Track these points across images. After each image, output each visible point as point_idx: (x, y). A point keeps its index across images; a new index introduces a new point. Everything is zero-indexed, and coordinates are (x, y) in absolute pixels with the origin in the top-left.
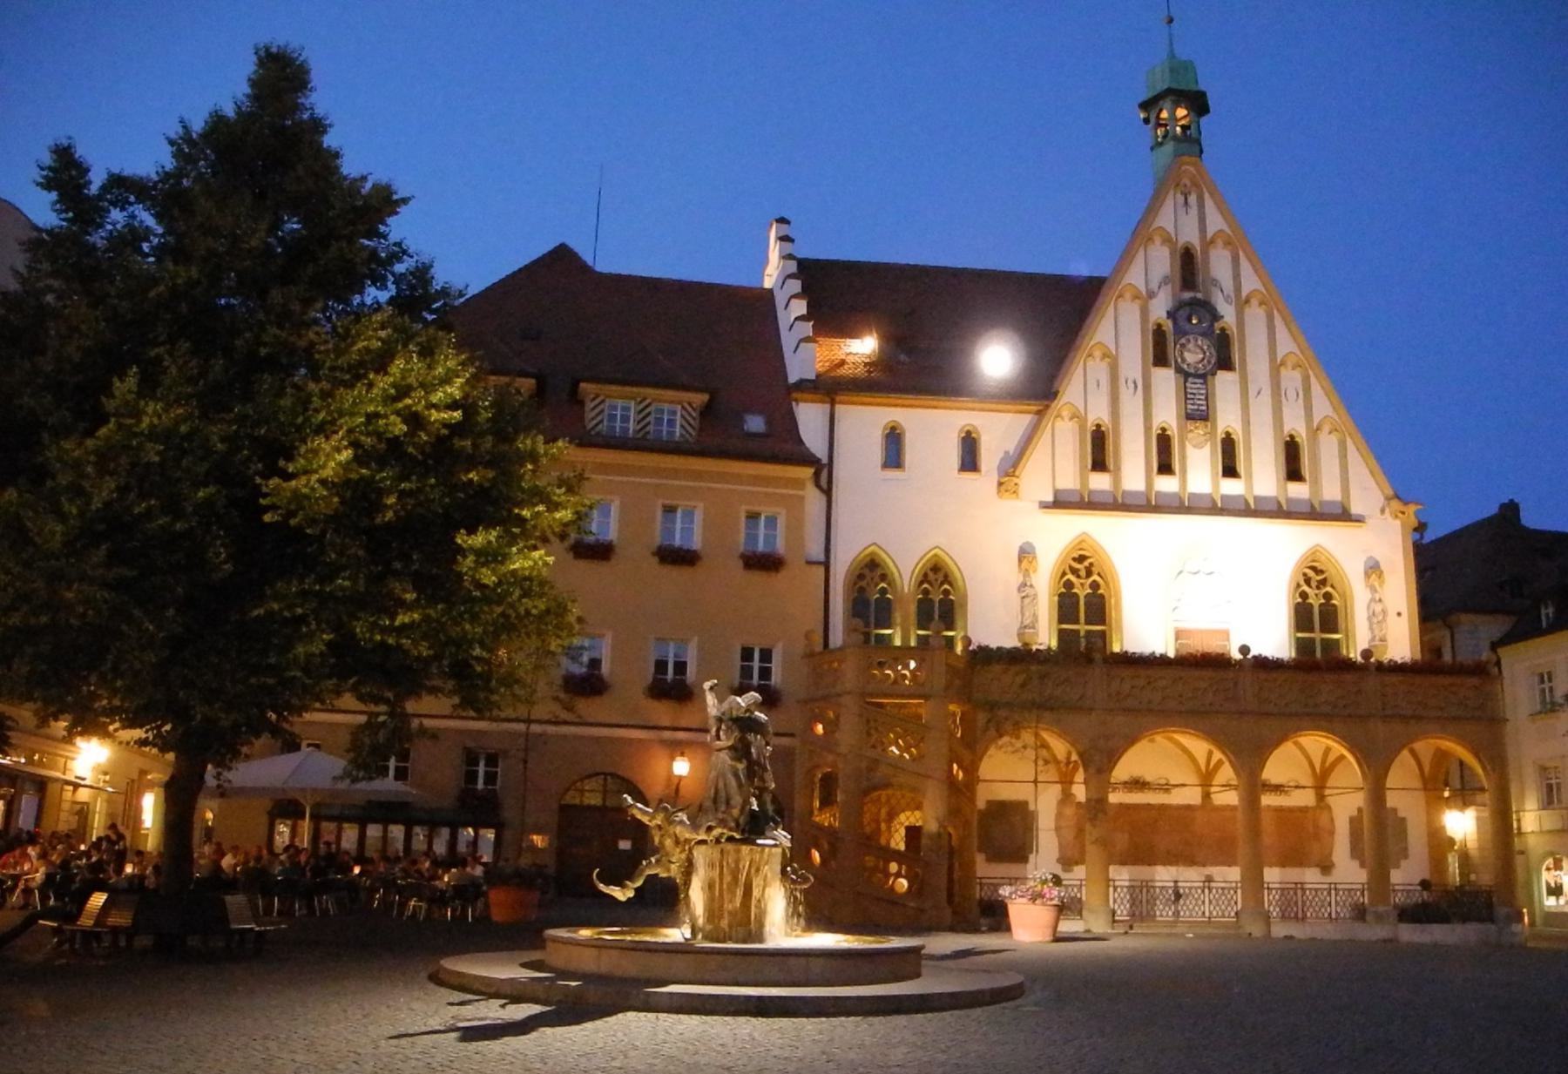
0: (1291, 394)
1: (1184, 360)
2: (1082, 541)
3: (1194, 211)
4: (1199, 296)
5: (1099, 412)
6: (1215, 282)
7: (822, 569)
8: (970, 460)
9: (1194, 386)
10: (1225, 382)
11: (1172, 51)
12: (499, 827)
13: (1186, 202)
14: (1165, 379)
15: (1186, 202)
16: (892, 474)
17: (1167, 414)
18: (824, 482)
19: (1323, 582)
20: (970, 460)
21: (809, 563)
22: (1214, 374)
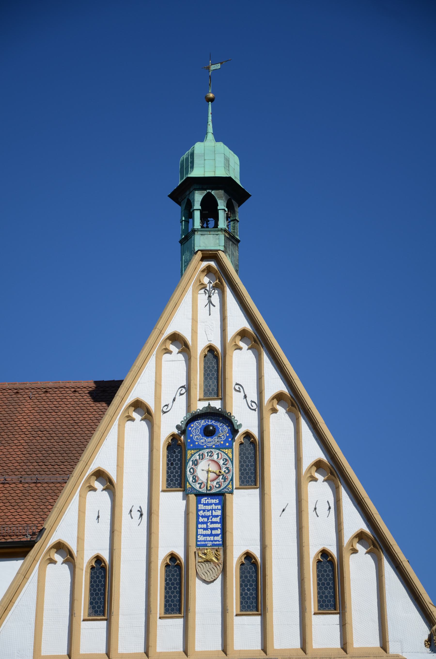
0: (323, 509)
1: (195, 479)
3: (216, 311)
4: (217, 404)
5: (97, 544)
6: (239, 388)
13: (210, 302)
14: (172, 505)
15: (210, 302)
22: (231, 493)
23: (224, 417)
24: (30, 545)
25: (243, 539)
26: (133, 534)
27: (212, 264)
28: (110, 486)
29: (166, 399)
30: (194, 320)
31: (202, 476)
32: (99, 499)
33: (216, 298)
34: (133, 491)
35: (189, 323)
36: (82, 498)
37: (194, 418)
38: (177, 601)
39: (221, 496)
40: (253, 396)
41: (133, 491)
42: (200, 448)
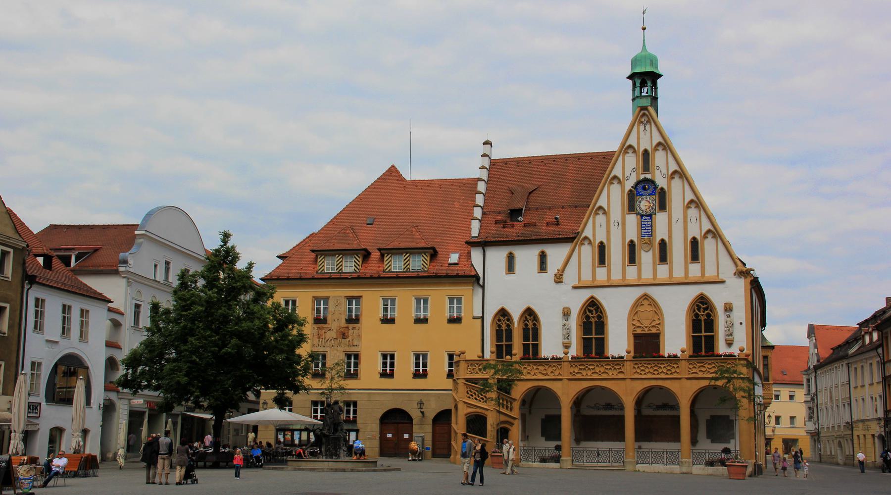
0: (694, 220)
2: (592, 297)
3: (648, 133)
4: (649, 176)
5: (601, 237)
7: (480, 320)
8: (543, 265)
11: (644, 46)
12: (357, 431)
17: (632, 233)
18: (481, 283)
19: (706, 309)
20: (543, 265)
21: (474, 318)
23: (652, 182)
24: (575, 238)
25: (661, 232)
26: (616, 232)
27: (646, 112)
29: (627, 174)
30: (638, 138)
31: (643, 208)
32: (601, 219)
35: (636, 140)
36: (594, 218)
38: (632, 260)
39: (650, 216)
40: (664, 171)
42: (642, 195)
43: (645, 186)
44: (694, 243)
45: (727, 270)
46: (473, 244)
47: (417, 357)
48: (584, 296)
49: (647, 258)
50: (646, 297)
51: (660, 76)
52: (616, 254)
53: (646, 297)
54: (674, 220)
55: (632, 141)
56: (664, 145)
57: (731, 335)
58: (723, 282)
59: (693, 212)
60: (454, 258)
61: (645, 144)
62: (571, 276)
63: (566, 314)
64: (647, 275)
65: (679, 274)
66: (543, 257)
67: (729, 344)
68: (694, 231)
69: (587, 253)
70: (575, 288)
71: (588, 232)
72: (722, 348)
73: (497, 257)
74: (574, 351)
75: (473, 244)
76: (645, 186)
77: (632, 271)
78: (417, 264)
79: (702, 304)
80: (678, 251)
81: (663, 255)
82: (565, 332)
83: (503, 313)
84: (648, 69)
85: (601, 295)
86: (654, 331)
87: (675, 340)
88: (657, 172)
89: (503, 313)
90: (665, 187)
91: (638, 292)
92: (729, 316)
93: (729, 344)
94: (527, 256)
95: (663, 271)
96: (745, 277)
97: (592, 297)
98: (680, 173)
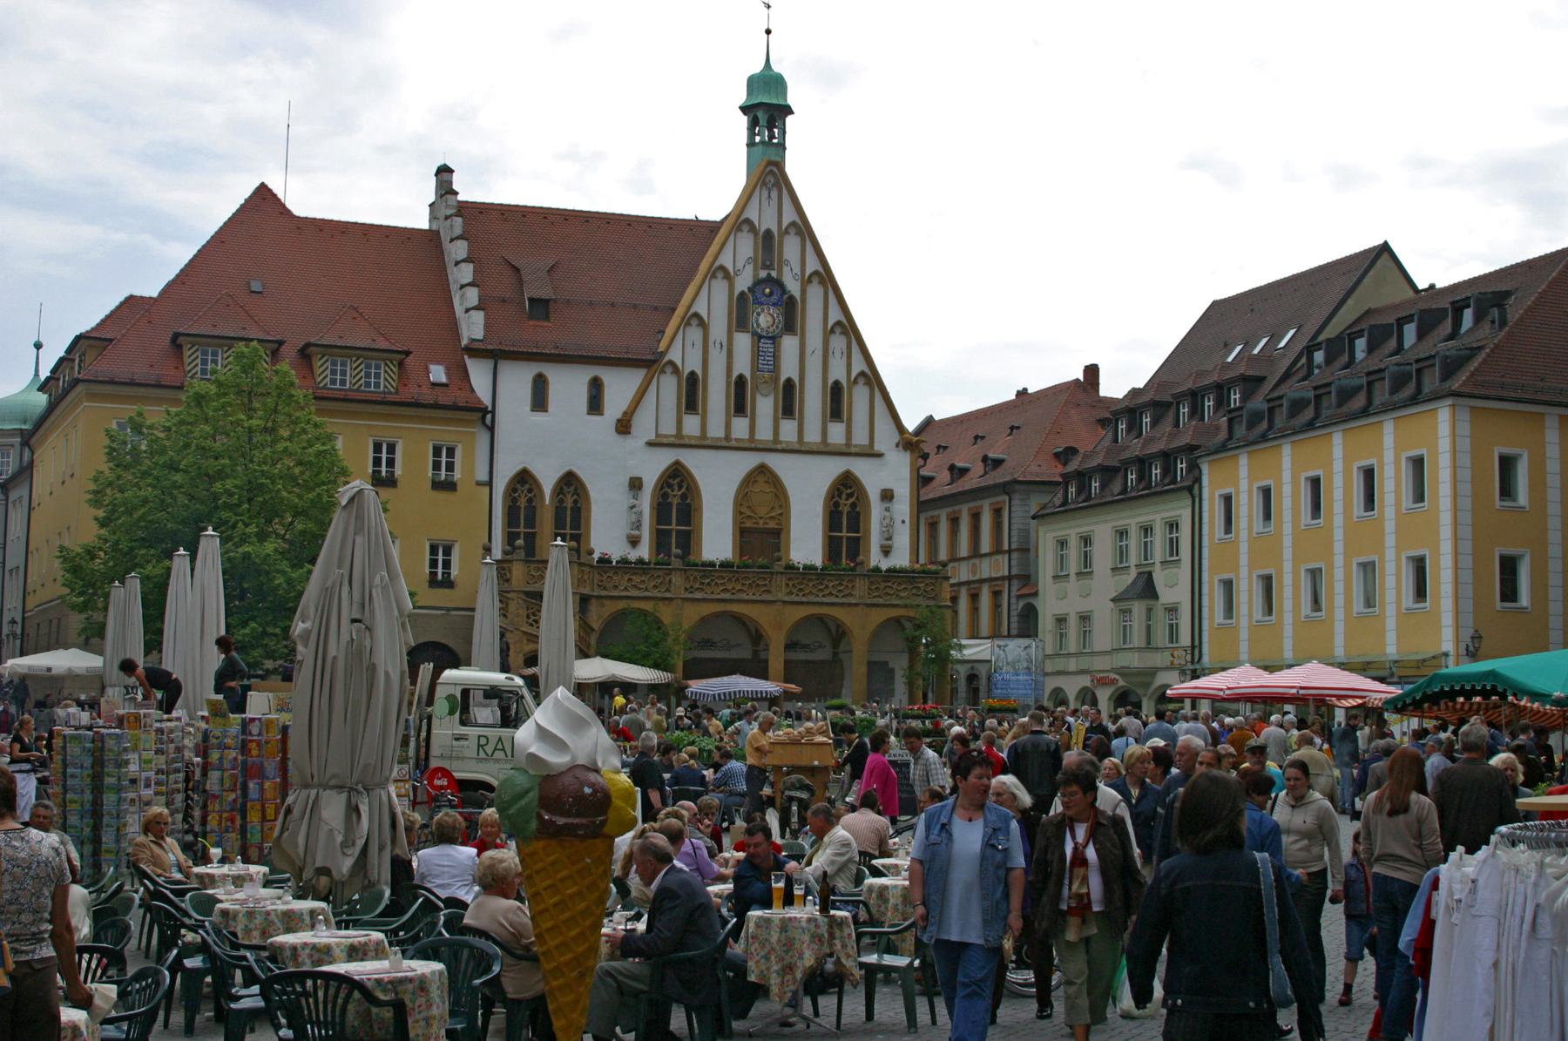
0: (838, 354)
2: (677, 463)
4: (774, 274)
5: (693, 364)
8: (595, 404)
9: (766, 346)
10: (789, 344)
16: (539, 417)
17: (743, 366)
19: (850, 496)
20: (595, 404)
21: (478, 484)
23: (779, 284)
25: (789, 369)
28: (703, 324)
29: (739, 265)
32: (695, 334)
33: (774, 194)
34: (719, 329)
37: (758, 283)
39: (774, 339)
40: (797, 270)
41: (719, 329)
43: (769, 288)
44: (836, 389)
45: (885, 439)
46: (474, 351)
47: (434, 550)
48: (662, 460)
49: (765, 406)
50: (762, 469)
51: (788, 110)
52: (717, 395)
53: (762, 469)
54: (808, 350)
55: (752, 213)
56: (803, 230)
57: (890, 538)
58: (880, 455)
59: (838, 342)
60: (438, 373)
61: (768, 222)
62: (644, 425)
63: (636, 485)
64: (764, 433)
65: (812, 436)
66: (596, 386)
67: (886, 551)
68: (838, 372)
69: (669, 388)
70: (650, 444)
71: (675, 355)
72: (875, 559)
73: (516, 382)
74: (644, 551)
75: (474, 351)
76: (769, 288)
77: (740, 427)
78: (385, 380)
79: (846, 486)
80: (813, 401)
81: (789, 402)
82: (634, 518)
83: (524, 478)
84: (774, 101)
85: (695, 462)
86: (772, 525)
87: (806, 544)
88: (786, 270)
89: (524, 478)
90: (797, 295)
91: (750, 461)
92: (887, 510)
93: (886, 551)
94: (568, 385)
95: (788, 429)
96: (912, 451)
97: (677, 463)
98: (825, 278)
